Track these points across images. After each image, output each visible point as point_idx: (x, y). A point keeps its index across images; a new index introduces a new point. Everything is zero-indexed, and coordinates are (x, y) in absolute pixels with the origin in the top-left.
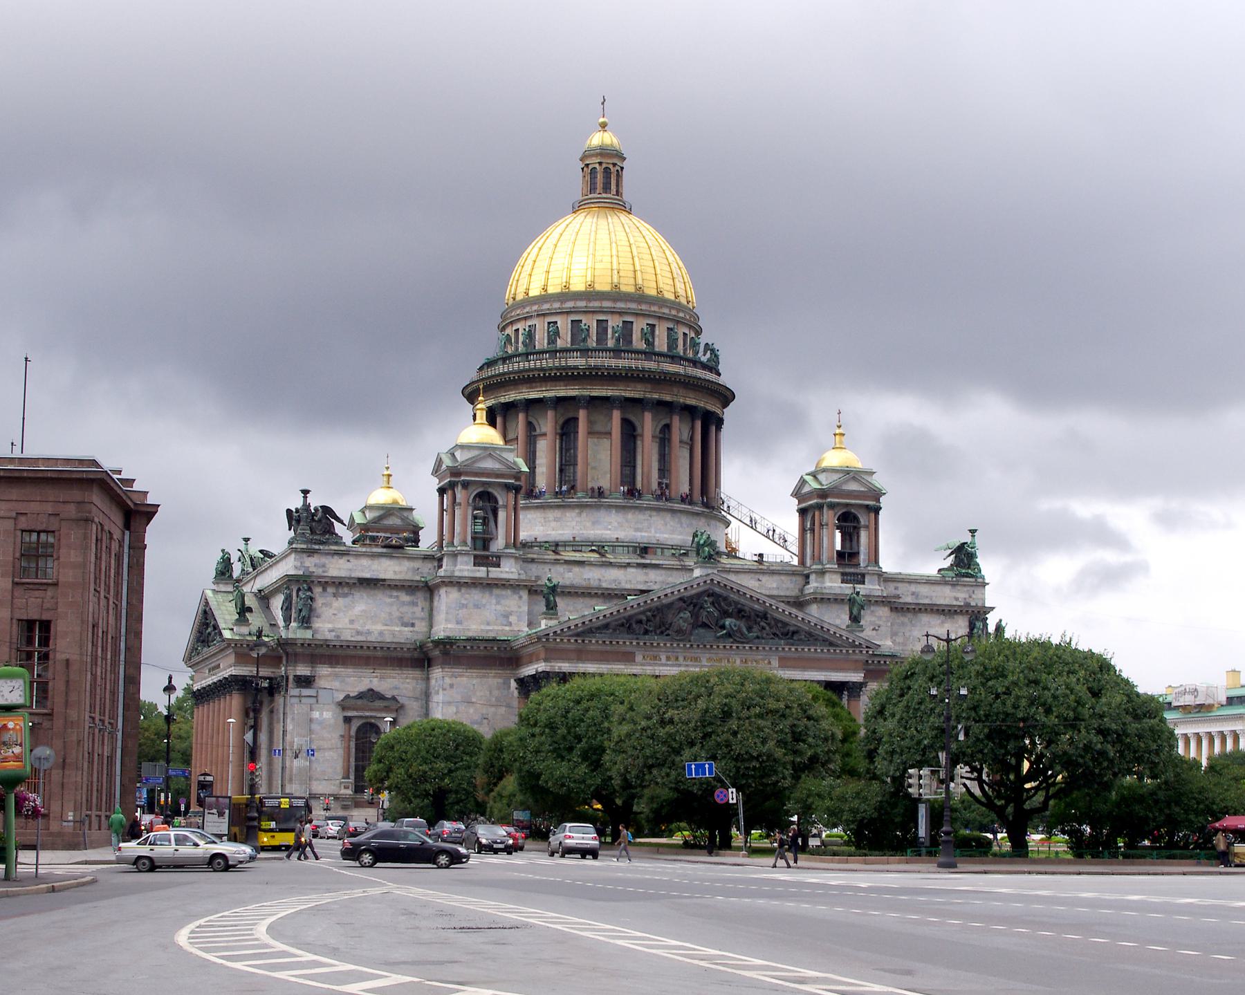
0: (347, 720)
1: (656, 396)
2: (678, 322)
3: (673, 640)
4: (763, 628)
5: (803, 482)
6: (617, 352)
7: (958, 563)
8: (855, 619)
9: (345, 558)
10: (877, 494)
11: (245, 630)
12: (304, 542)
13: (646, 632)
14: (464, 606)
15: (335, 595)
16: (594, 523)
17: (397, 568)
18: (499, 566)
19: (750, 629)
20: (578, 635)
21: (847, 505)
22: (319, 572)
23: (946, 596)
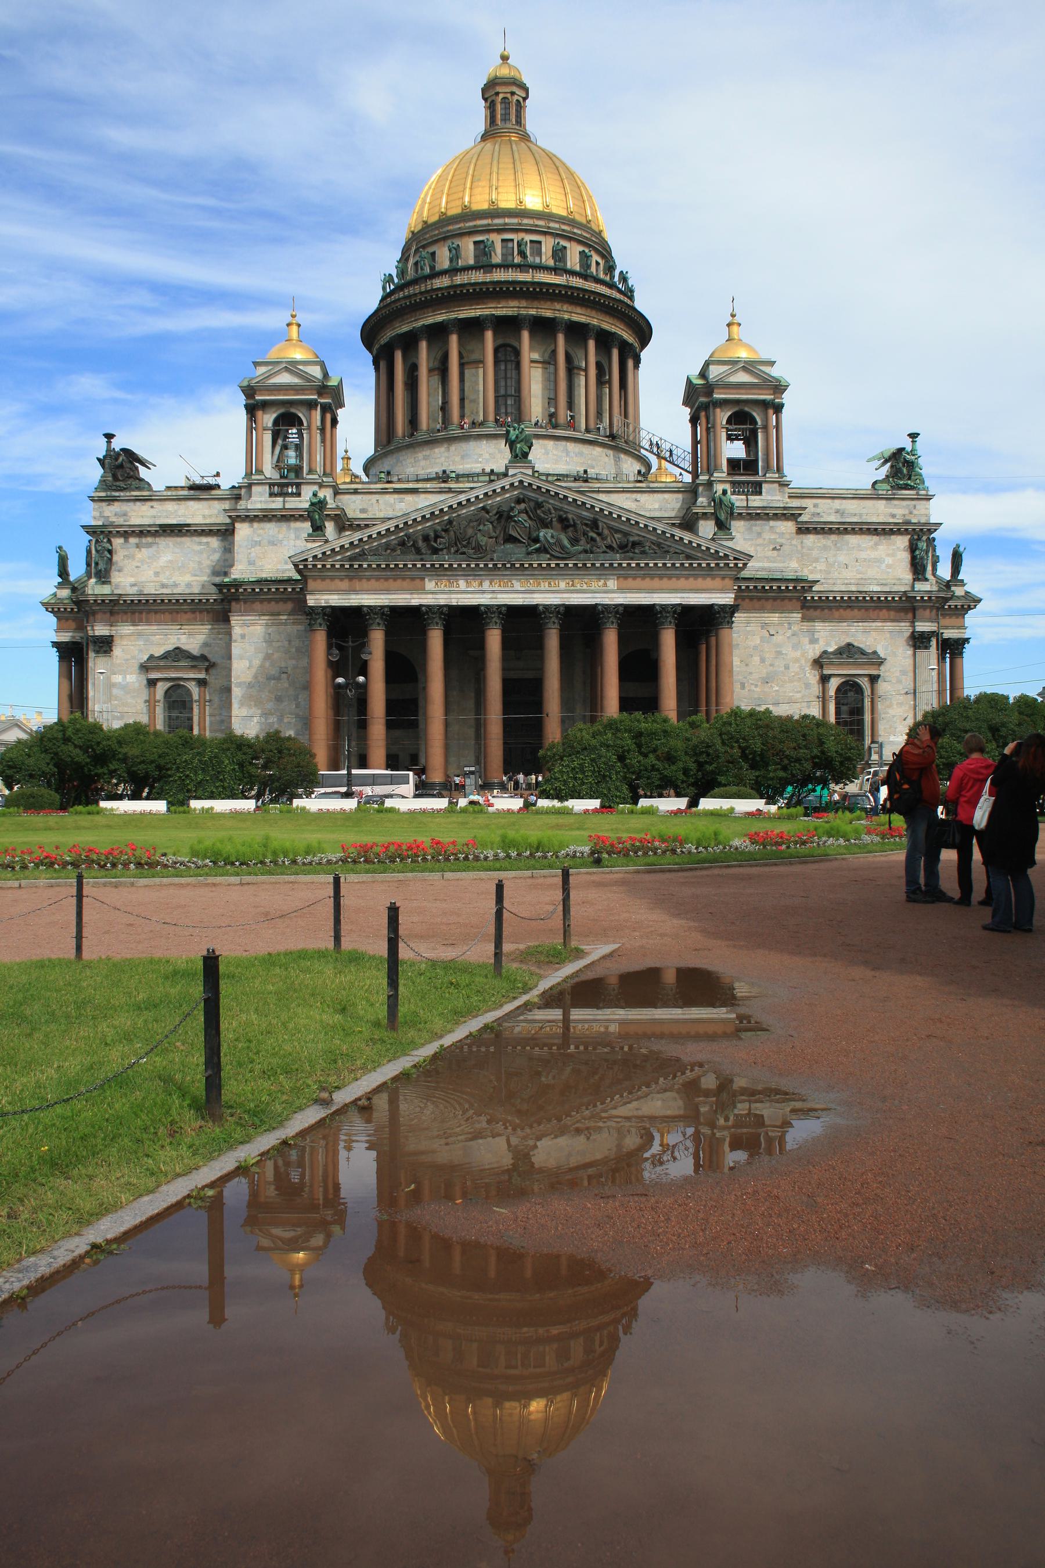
0: (152, 683)
1: (533, 312)
2: (570, 239)
3: (470, 558)
4: (593, 539)
5: (689, 381)
6: (490, 267)
7: (895, 473)
8: (722, 526)
9: (150, 504)
10: (779, 388)
11: (65, 593)
12: (105, 490)
13: (435, 551)
14: (259, 543)
15: (138, 546)
16: (463, 458)
17: (207, 512)
18: (299, 495)
19: (574, 541)
20: (351, 559)
21: (737, 402)
22: (120, 521)
23: (879, 512)
